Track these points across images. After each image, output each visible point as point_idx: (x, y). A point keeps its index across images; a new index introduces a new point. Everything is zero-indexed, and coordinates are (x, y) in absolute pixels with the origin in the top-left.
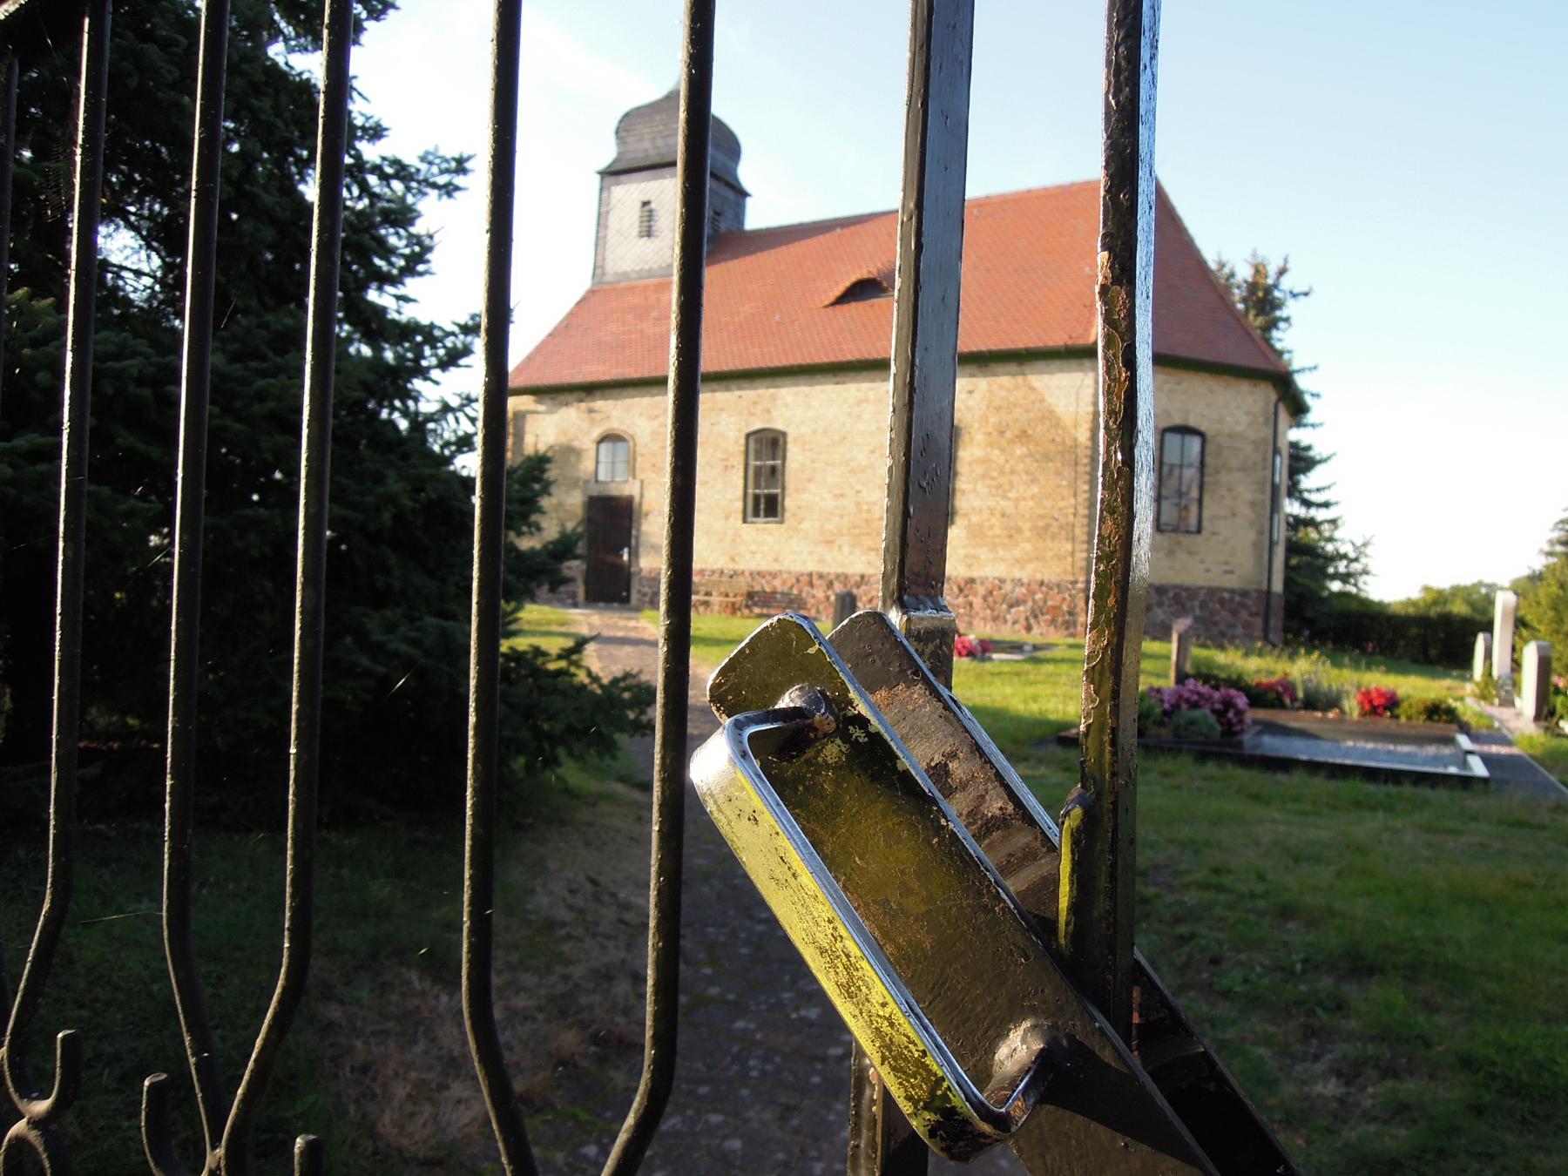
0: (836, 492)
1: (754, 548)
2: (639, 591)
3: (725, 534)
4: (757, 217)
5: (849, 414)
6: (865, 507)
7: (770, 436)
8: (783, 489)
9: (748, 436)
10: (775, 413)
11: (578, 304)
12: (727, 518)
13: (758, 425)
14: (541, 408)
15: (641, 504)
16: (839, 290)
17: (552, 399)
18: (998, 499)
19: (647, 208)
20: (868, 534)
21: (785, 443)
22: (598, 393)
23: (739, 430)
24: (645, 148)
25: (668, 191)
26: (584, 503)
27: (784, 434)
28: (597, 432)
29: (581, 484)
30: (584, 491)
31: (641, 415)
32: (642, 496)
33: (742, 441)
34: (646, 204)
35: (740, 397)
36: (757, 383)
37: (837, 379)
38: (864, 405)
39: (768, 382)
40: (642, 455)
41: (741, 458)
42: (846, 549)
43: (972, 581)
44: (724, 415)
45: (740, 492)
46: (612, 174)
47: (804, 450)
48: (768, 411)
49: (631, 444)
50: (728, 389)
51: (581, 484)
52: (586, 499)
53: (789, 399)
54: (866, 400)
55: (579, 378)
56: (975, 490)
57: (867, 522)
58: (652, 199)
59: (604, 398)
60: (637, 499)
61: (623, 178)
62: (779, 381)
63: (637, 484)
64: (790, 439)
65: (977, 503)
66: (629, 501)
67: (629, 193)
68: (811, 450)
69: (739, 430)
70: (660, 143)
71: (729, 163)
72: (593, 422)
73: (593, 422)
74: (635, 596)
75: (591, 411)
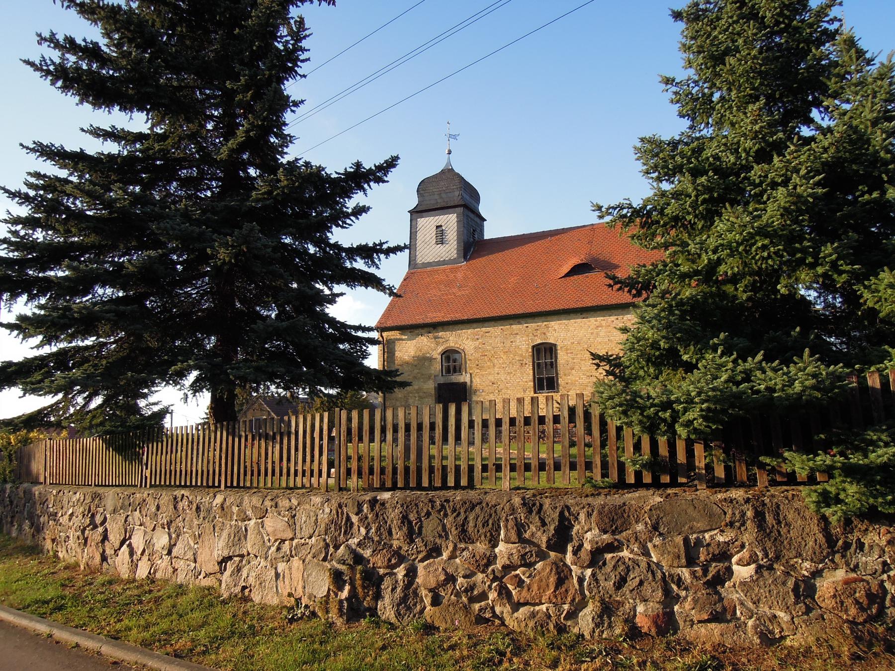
0: (588, 374)
4: (490, 232)
5: (592, 333)
7: (548, 346)
8: (557, 374)
9: (533, 347)
10: (548, 334)
11: (405, 280)
12: (524, 391)
13: (539, 341)
14: (404, 337)
15: (471, 386)
16: (566, 269)
19: (441, 229)
21: (556, 350)
22: (440, 328)
23: (528, 345)
24: (433, 200)
25: (450, 221)
26: (435, 387)
27: (555, 345)
28: (440, 349)
30: (435, 381)
31: (468, 338)
32: (471, 381)
33: (530, 350)
34: (437, 227)
36: (536, 319)
39: (543, 318)
40: (470, 360)
41: (531, 360)
44: (518, 337)
45: (531, 377)
46: (416, 213)
47: (567, 353)
48: (545, 334)
49: (463, 355)
50: (520, 323)
51: (433, 377)
53: (556, 327)
54: (602, 326)
55: (428, 321)
58: (443, 224)
60: (469, 383)
61: (424, 214)
62: (549, 318)
63: (468, 375)
64: (559, 348)
66: (465, 384)
67: (427, 224)
68: (572, 353)
69: (528, 345)
70: (444, 195)
71: (475, 204)
72: (438, 344)
73: (438, 344)
75: (435, 338)
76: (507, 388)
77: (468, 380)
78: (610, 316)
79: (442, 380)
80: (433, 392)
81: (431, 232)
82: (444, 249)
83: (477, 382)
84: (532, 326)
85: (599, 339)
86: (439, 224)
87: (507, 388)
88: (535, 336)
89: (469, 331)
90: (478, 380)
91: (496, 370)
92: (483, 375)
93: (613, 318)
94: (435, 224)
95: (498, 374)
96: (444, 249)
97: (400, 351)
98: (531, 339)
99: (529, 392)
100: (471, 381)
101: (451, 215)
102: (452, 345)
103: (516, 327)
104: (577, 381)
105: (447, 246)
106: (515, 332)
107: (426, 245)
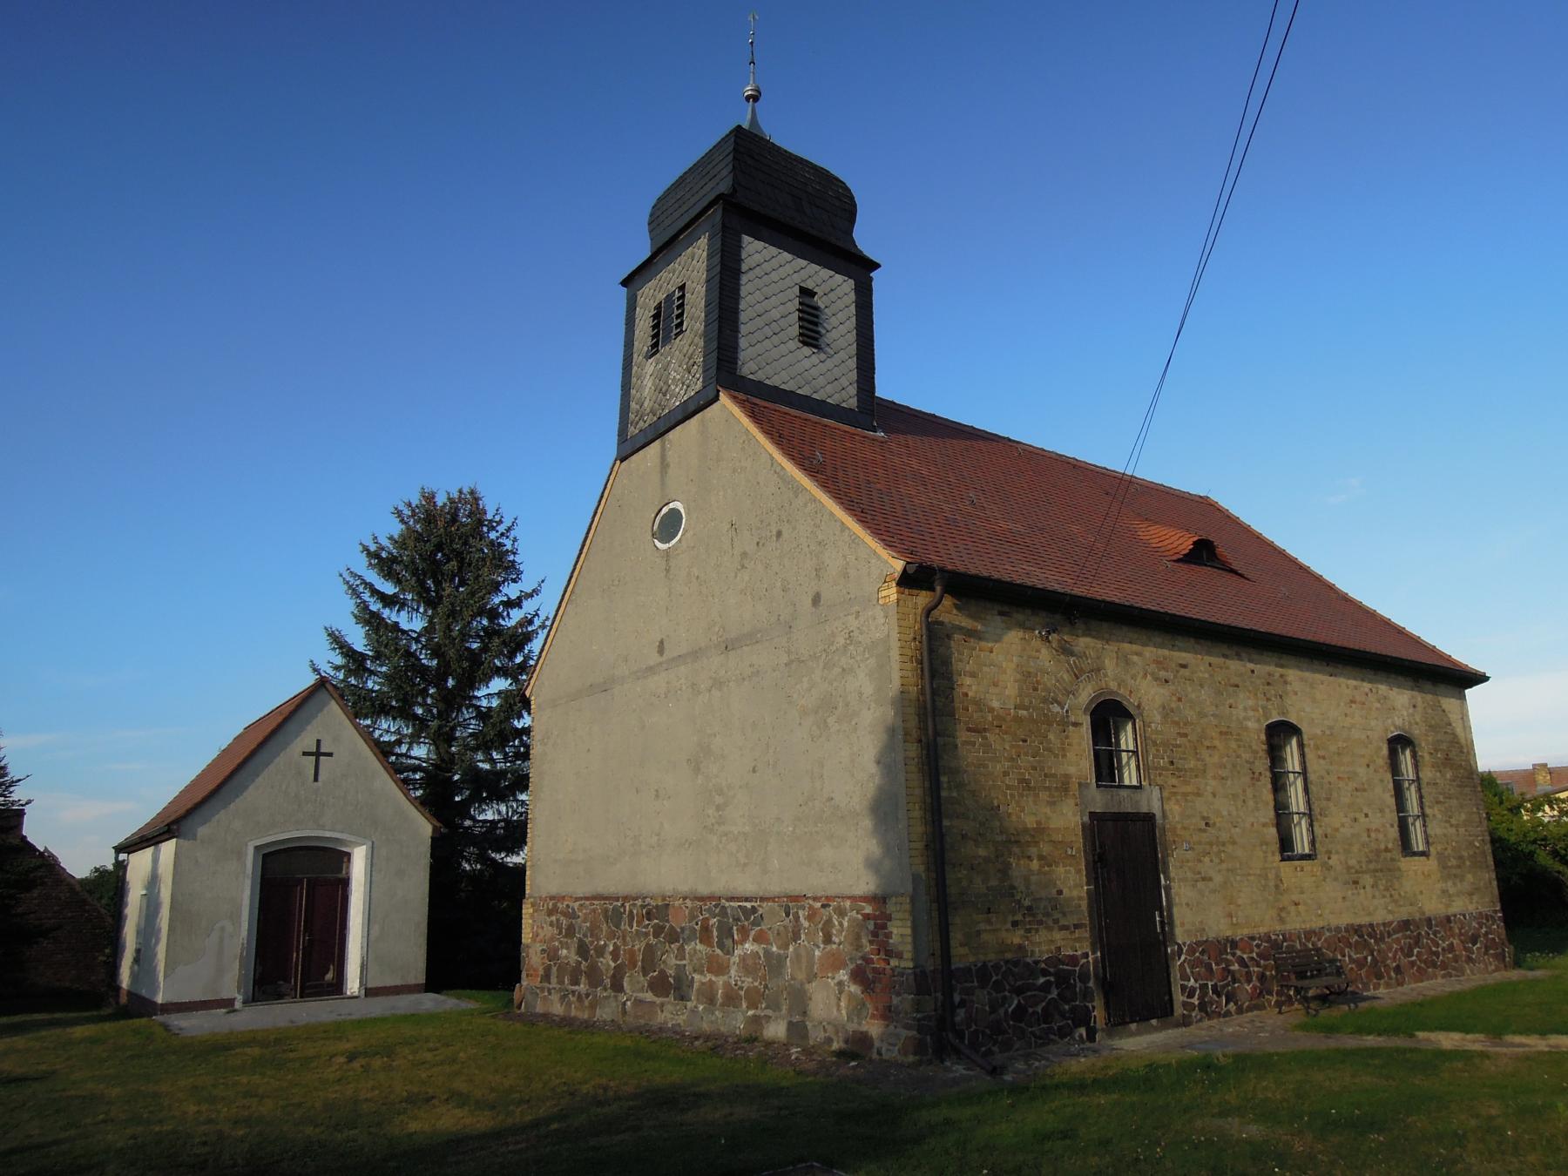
1: (1295, 897)
2: (1183, 988)
3: (1266, 878)
6: (1373, 835)
13: (1275, 718)
17: (1001, 614)
18: (1447, 825)
20: (1381, 871)
26: (1083, 825)
28: (1086, 694)
29: (1074, 787)
33: (1263, 737)
35: (1253, 671)
37: (1330, 669)
38: (1354, 705)
42: (1368, 888)
43: (1448, 919)
48: (1281, 697)
50: (1239, 656)
52: (1086, 819)
56: (1434, 815)
57: (1378, 852)
59: (1087, 633)
63: (1156, 792)
65: (1439, 831)
66: (1149, 818)
68: (1324, 758)
69: (1258, 721)
74: (1179, 998)
76: (1234, 843)
77: (1156, 808)
78: (1363, 680)
79: (1099, 801)
80: (1079, 842)
81: (782, 297)
82: (823, 368)
83: (1174, 809)
84: (1265, 668)
85: (1356, 734)
86: (809, 285)
87: (1234, 843)
88: (1268, 700)
89: (1150, 652)
90: (1176, 808)
91: (1212, 784)
92: (1185, 795)
93: (1366, 686)
94: (797, 278)
95: (1214, 795)
96: (823, 368)
97: (973, 675)
98: (1264, 708)
99: (1273, 854)
100: (1164, 812)
101: (839, 278)
102: (1113, 686)
103: (1237, 667)
104: (1337, 830)
105: (829, 363)
106: (1235, 680)
107: (768, 331)
